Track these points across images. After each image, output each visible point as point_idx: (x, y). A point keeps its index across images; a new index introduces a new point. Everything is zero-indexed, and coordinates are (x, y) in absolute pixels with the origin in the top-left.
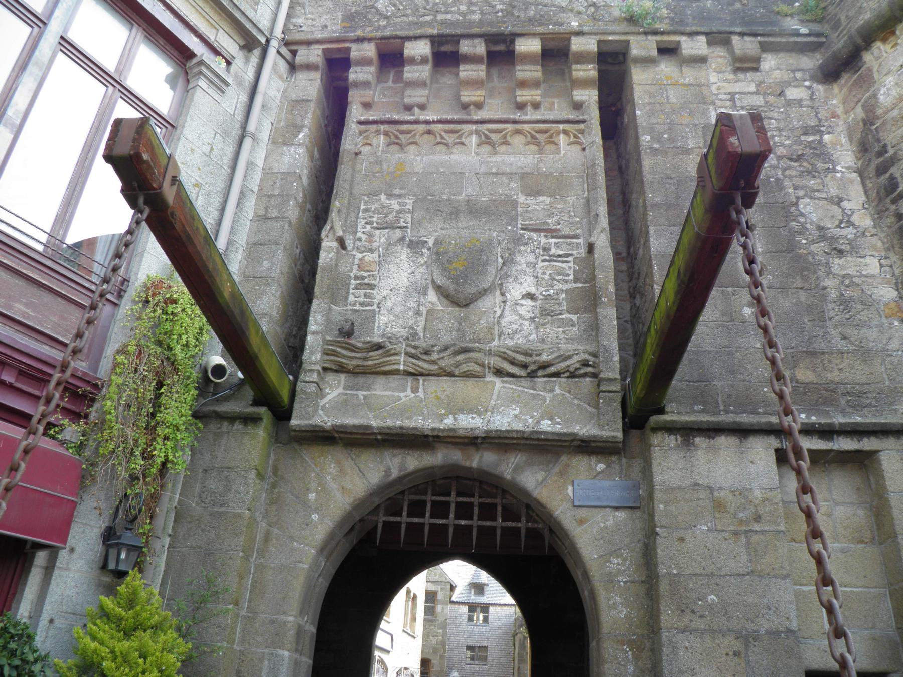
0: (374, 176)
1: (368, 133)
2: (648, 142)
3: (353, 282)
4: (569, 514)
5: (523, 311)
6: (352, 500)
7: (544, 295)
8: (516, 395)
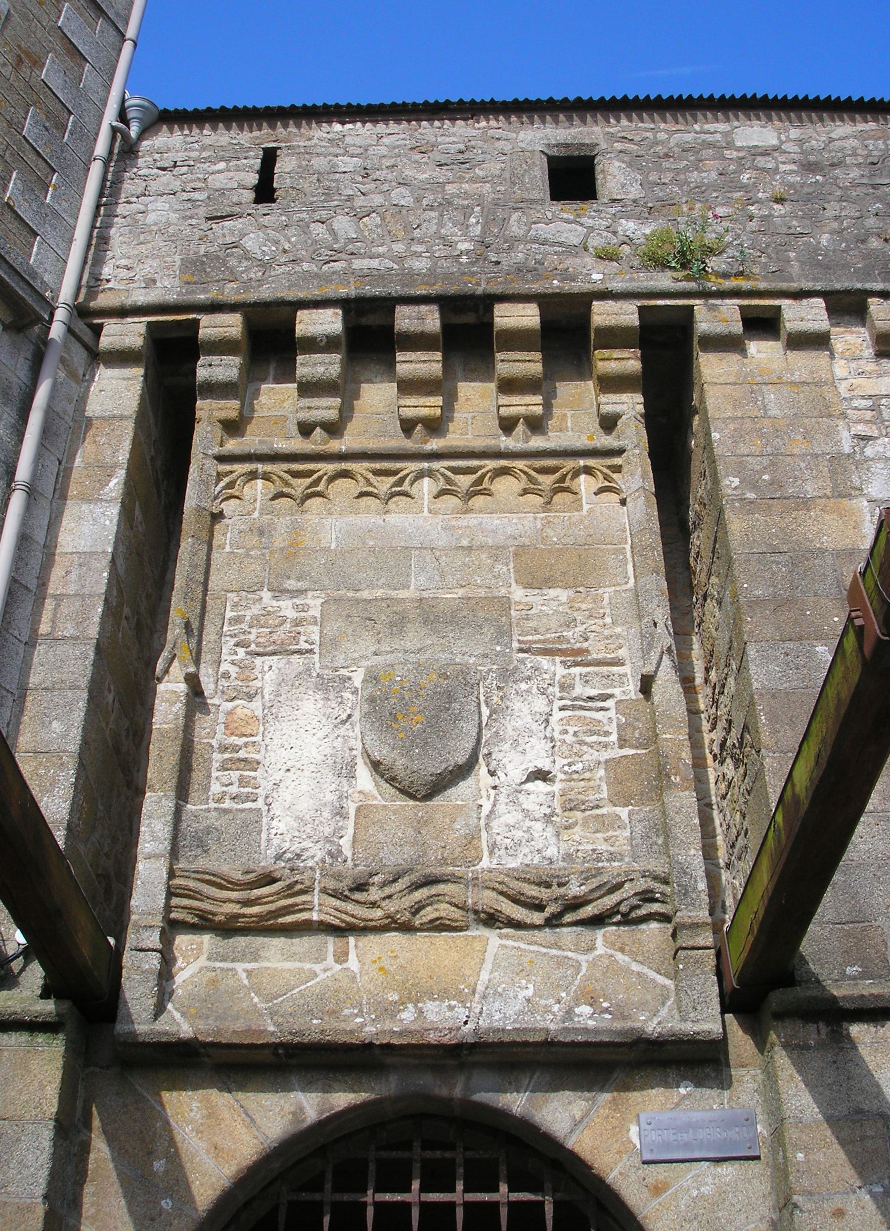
0: (248, 555)
1: (234, 475)
2: (735, 488)
3: (216, 756)
4: (633, 1177)
5: (528, 803)
6: (234, 1169)
7: (566, 773)
8: (525, 960)
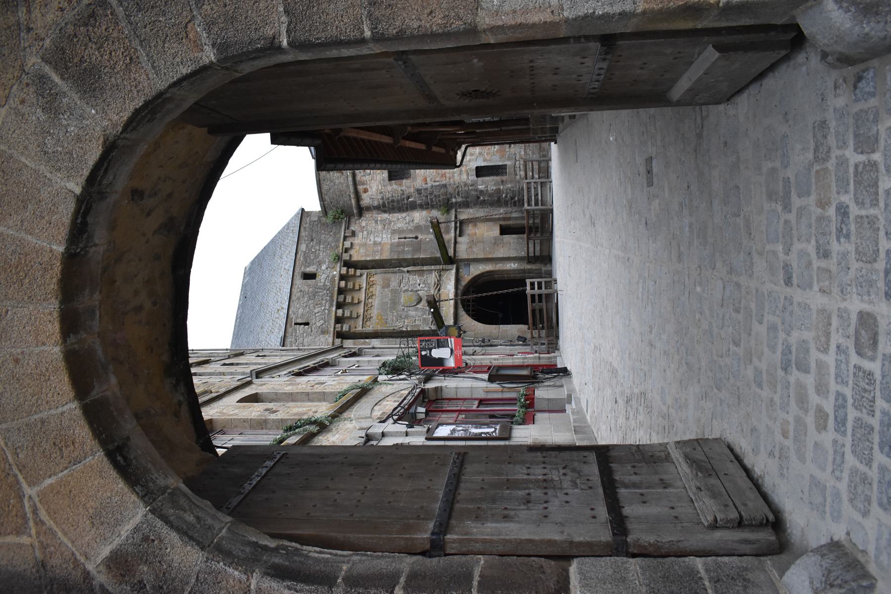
5: (424, 286)
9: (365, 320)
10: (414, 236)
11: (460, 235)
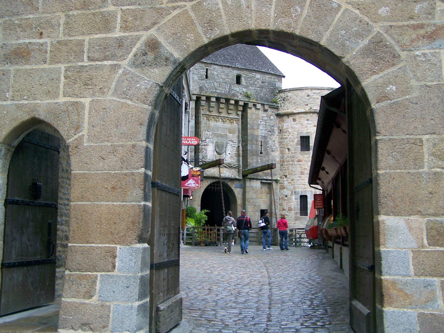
9: (207, 116)
10: (262, 152)
11: (261, 182)
